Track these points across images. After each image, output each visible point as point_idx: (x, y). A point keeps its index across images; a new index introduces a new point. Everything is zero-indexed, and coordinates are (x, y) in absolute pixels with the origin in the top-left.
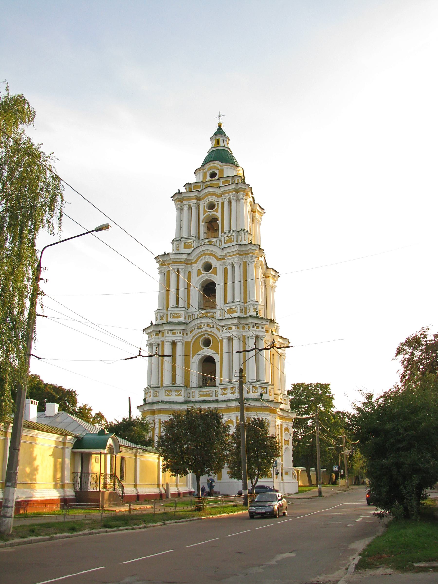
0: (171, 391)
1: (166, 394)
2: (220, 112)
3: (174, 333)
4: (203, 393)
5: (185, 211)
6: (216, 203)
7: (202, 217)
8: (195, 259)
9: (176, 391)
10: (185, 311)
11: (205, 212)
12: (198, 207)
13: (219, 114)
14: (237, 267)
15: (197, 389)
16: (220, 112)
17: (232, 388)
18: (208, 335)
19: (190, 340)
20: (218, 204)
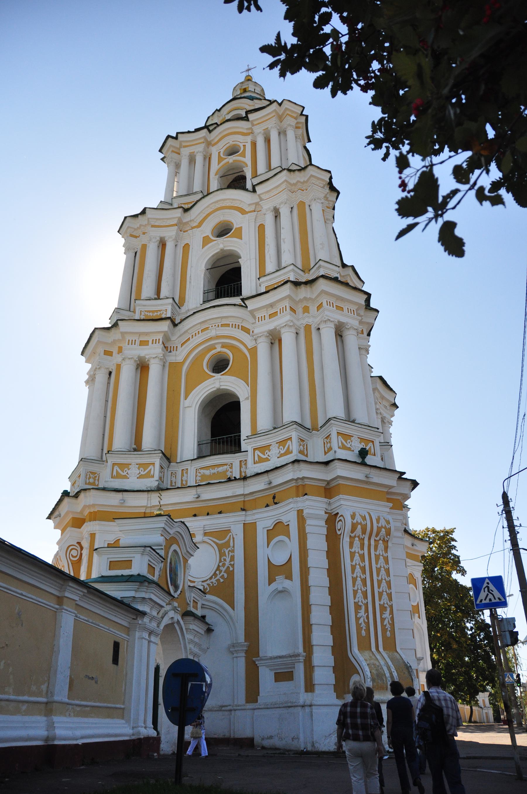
0: (127, 466)
1: (115, 473)
2: (248, 66)
3: (144, 343)
4: (207, 472)
5: (185, 163)
6: (241, 145)
7: (215, 166)
8: (198, 221)
9: (140, 465)
10: (172, 305)
11: (220, 159)
12: (208, 159)
13: (247, 68)
14: (284, 212)
15: (193, 462)
16: (248, 66)
17: (282, 443)
18: (223, 347)
19: (180, 359)
20: (244, 146)
